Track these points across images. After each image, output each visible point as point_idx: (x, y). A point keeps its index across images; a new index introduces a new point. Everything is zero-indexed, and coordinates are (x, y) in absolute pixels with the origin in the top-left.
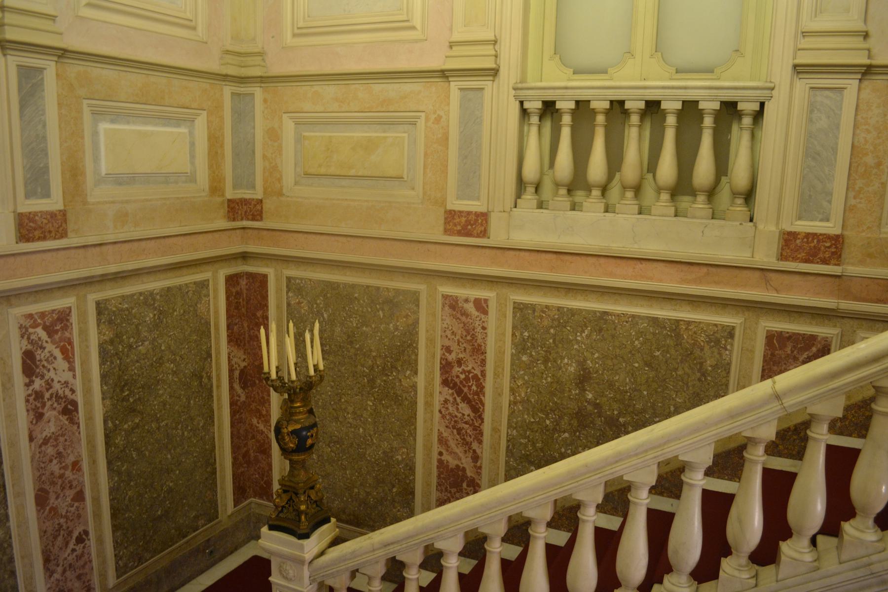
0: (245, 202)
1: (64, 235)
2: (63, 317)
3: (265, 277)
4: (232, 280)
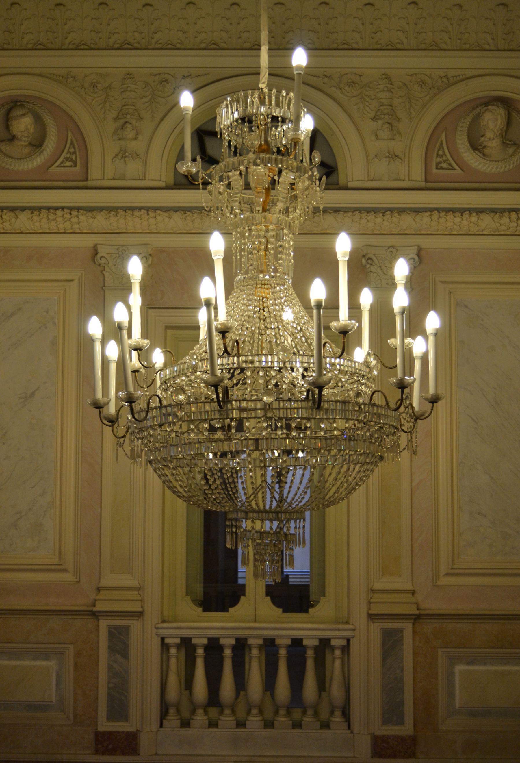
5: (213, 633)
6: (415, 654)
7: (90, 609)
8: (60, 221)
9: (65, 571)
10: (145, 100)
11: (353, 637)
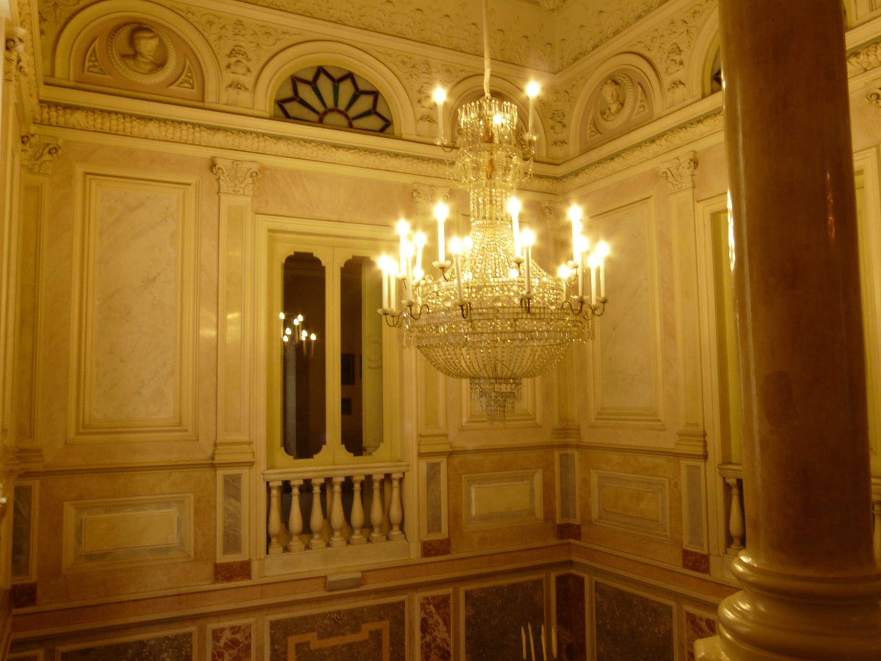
0: (568, 526)
1: (447, 552)
2: (445, 599)
3: (583, 579)
4: (560, 580)
5: (307, 476)
6: (448, 480)
7: (210, 462)
8: (184, 133)
9: (186, 431)
10: (252, 45)
11: (408, 470)
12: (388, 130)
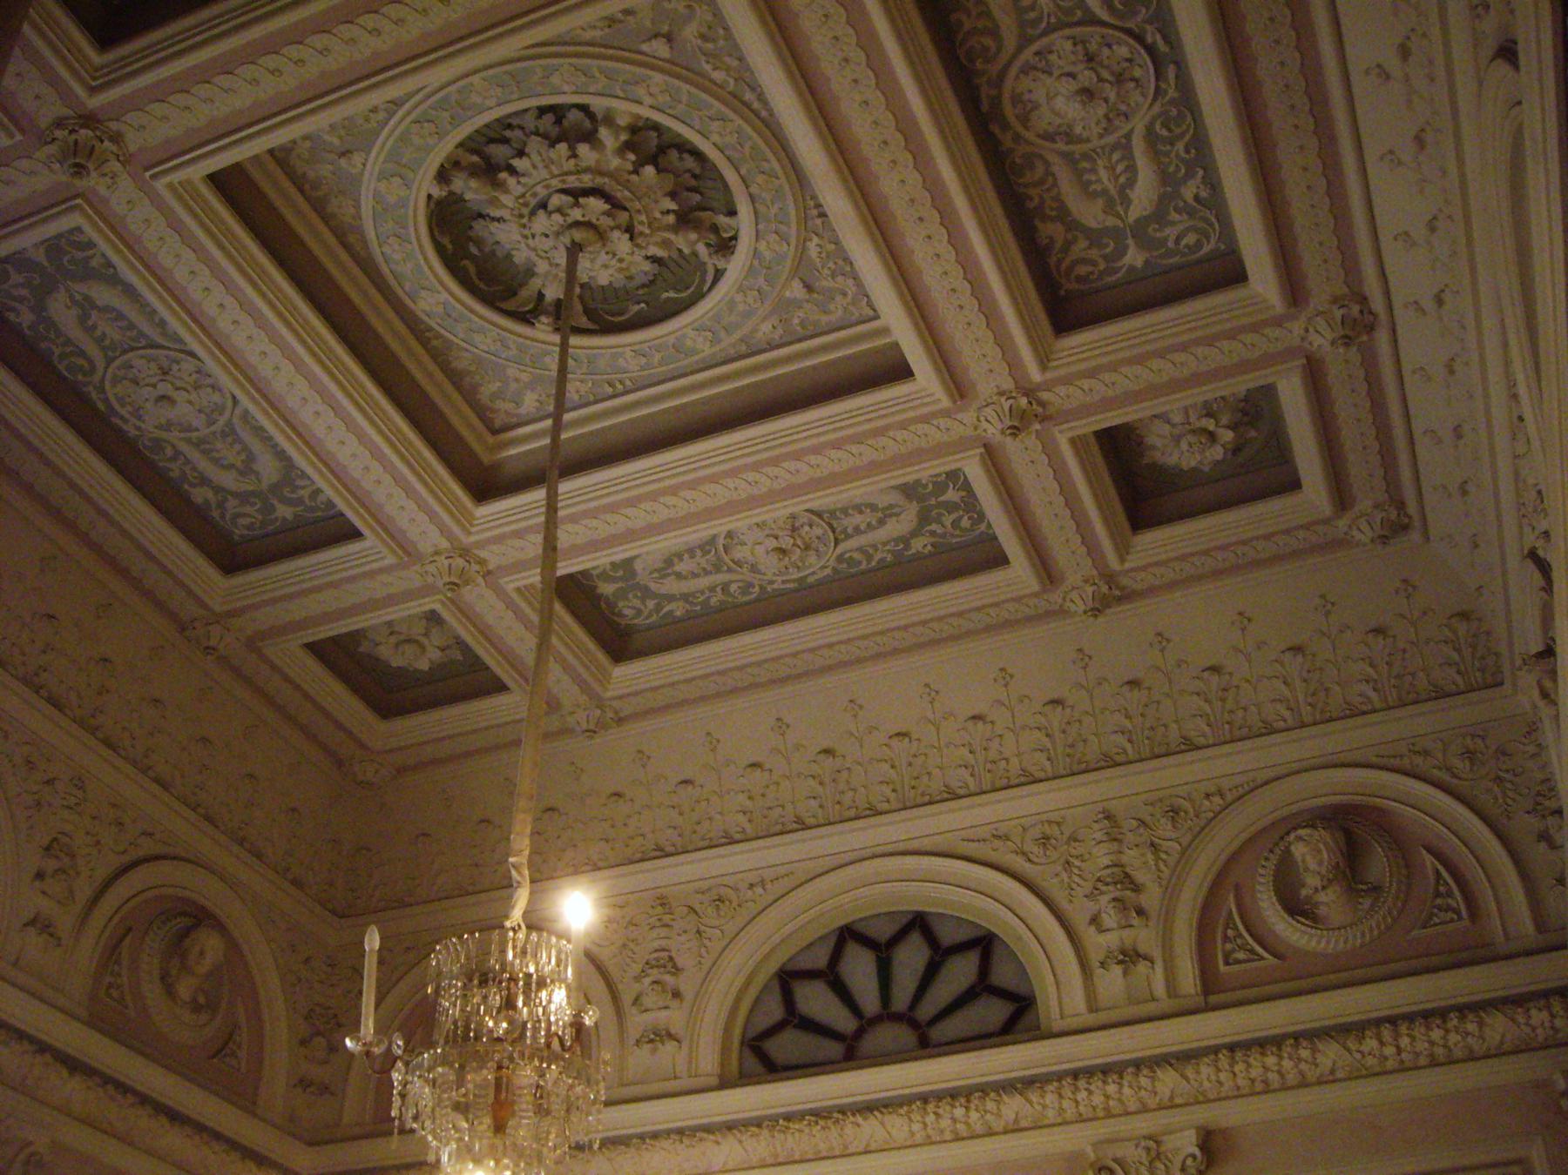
12: (1026, 1021)
